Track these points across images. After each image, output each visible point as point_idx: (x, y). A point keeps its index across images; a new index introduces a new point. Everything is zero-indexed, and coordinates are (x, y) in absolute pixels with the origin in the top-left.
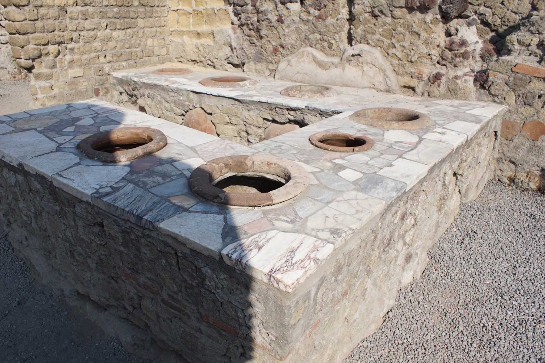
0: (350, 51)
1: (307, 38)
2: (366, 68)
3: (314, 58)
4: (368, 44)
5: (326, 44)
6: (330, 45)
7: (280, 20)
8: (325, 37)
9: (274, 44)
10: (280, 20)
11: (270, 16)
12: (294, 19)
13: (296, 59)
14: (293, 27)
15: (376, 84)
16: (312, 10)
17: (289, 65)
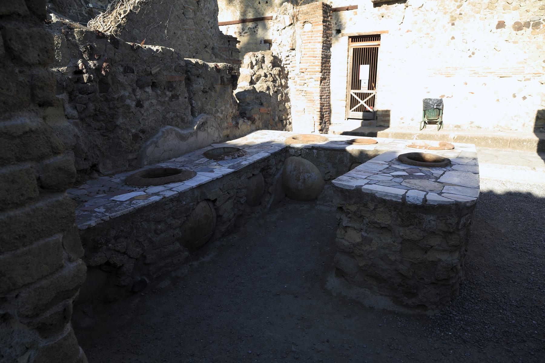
0: (199, 121)
1: (164, 118)
2: (209, 130)
3: (177, 134)
4: (205, 113)
5: (179, 120)
6: (183, 120)
7: (139, 104)
8: (178, 114)
9: (133, 131)
10: (139, 104)
11: (128, 102)
12: (152, 101)
13: (163, 139)
14: (151, 111)
15: (215, 139)
16: (168, 93)
17: (156, 146)
